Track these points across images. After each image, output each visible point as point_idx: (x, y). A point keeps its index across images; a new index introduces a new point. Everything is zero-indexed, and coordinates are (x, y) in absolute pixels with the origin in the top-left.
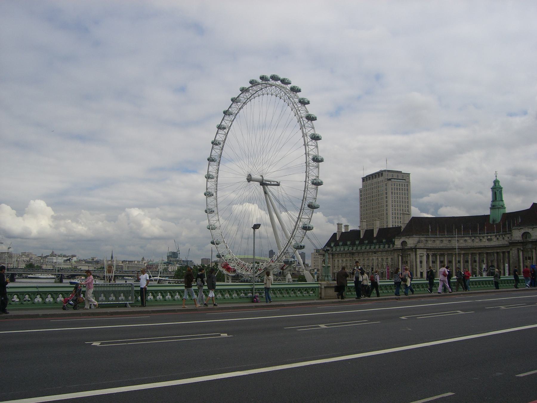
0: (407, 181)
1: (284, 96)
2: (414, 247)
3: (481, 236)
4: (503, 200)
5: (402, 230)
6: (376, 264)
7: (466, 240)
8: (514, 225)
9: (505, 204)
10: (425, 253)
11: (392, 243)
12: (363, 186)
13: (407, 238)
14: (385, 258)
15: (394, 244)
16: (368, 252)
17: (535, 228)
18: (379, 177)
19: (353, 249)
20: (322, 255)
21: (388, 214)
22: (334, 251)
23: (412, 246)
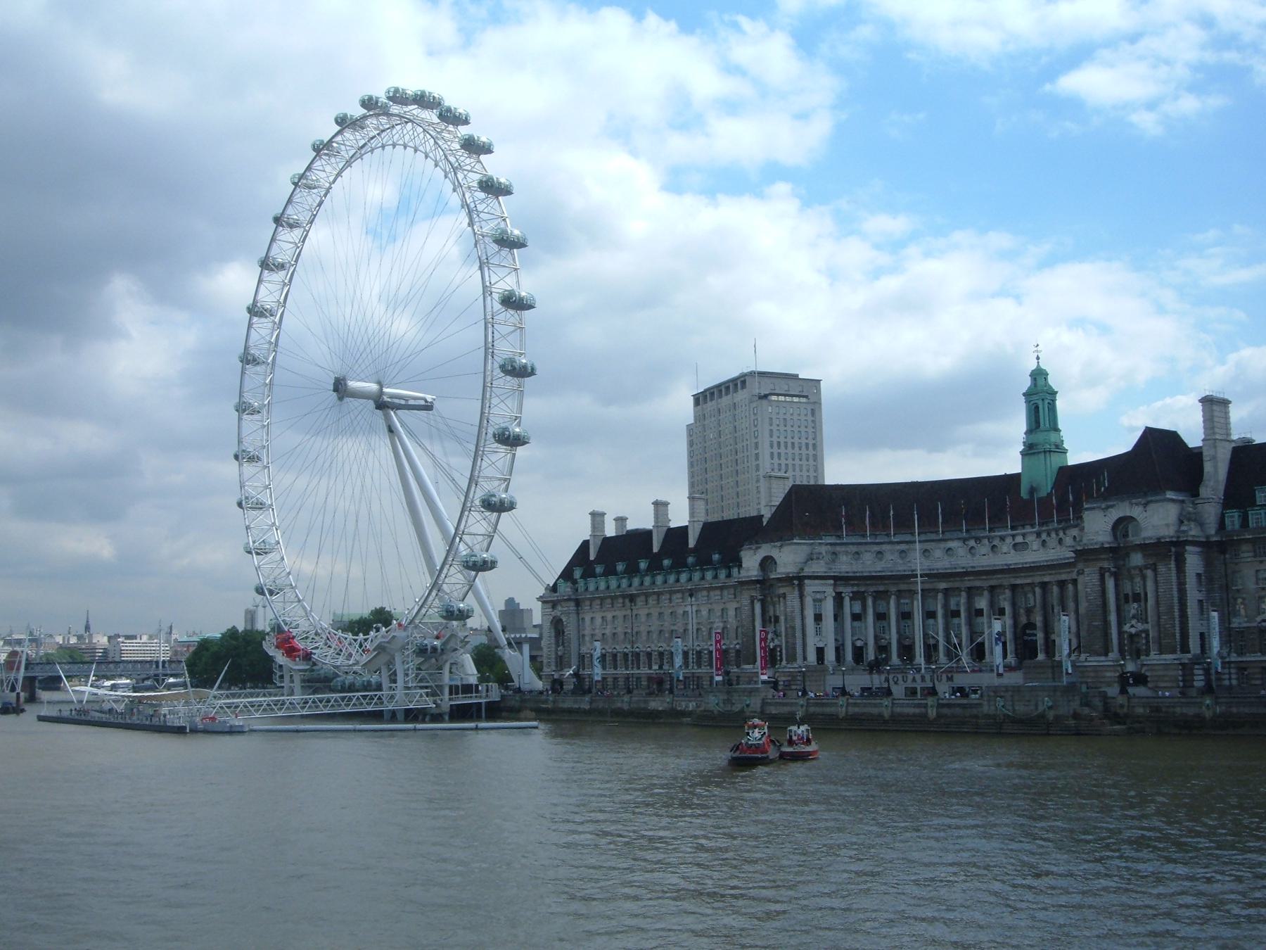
0: (812, 400)
3: (996, 536)
4: (1060, 427)
5: (764, 524)
6: (695, 627)
7: (950, 549)
8: (1090, 497)
9: (1064, 439)
10: (830, 591)
12: (695, 417)
13: (775, 546)
15: (740, 566)
16: (671, 593)
17: (1151, 501)
18: (736, 390)
19: (630, 586)
23: (788, 571)
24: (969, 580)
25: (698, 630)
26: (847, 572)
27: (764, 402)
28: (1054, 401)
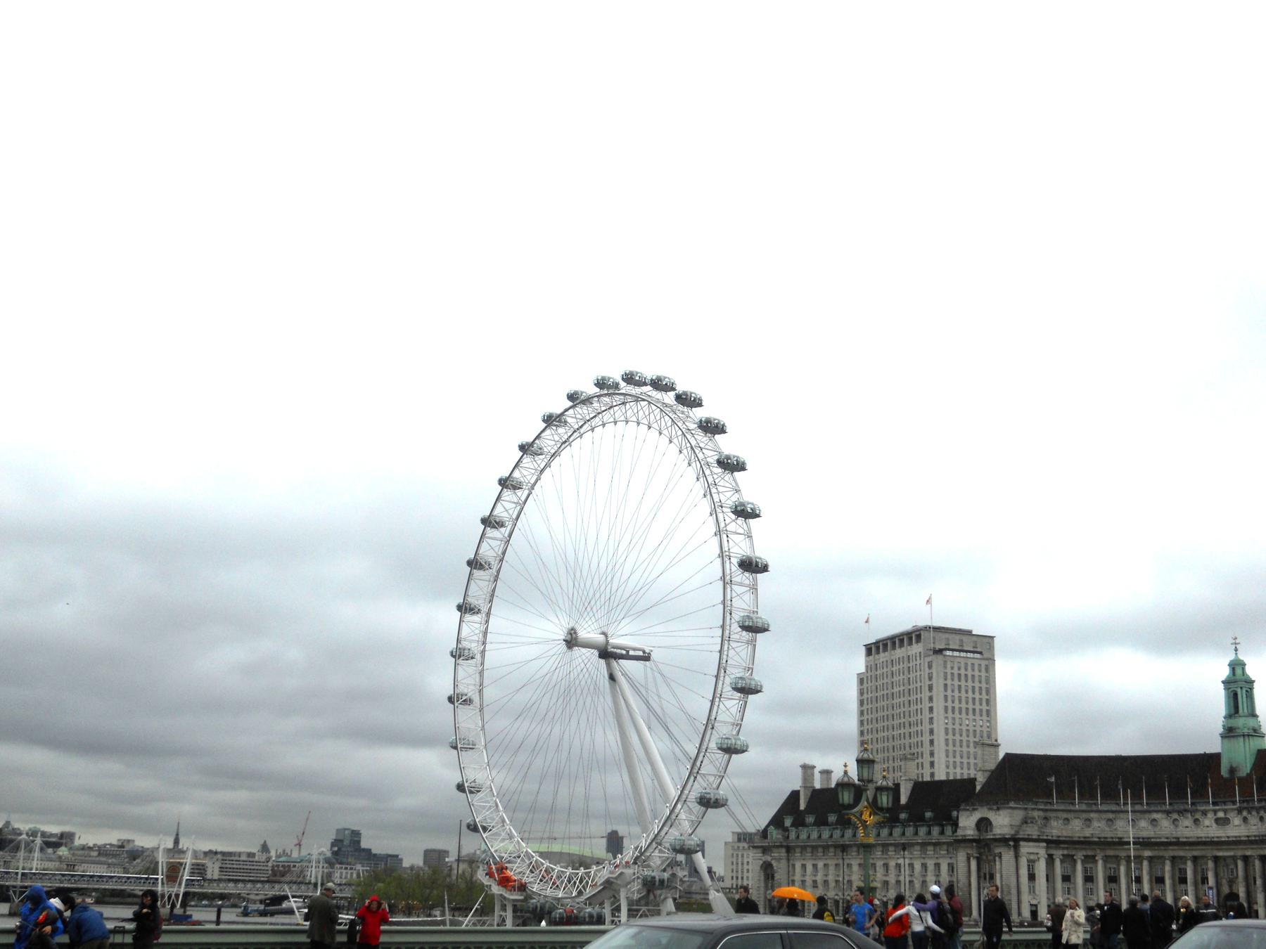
0: (986, 655)
1: (670, 429)
2: (1012, 835)
4: (1258, 712)
5: (978, 788)
6: (907, 879)
7: (1154, 820)
9: (1261, 724)
10: (1042, 853)
11: (951, 822)
12: (867, 667)
13: (990, 809)
14: (931, 864)
16: (885, 847)
20: (760, 850)
21: (936, 743)
22: (792, 840)
23: (1006, 832)
24: (1173, 850)
25: (910, 881)
26: (1059, 837)
27: (940, 657)
28: (1251, 689)
